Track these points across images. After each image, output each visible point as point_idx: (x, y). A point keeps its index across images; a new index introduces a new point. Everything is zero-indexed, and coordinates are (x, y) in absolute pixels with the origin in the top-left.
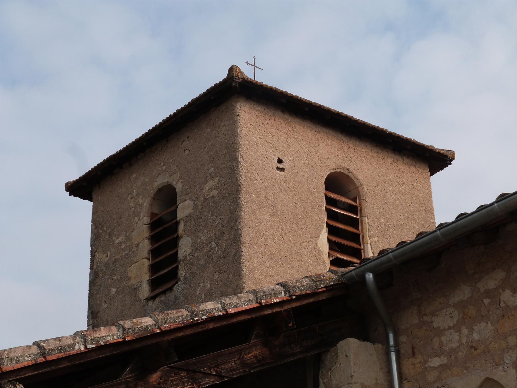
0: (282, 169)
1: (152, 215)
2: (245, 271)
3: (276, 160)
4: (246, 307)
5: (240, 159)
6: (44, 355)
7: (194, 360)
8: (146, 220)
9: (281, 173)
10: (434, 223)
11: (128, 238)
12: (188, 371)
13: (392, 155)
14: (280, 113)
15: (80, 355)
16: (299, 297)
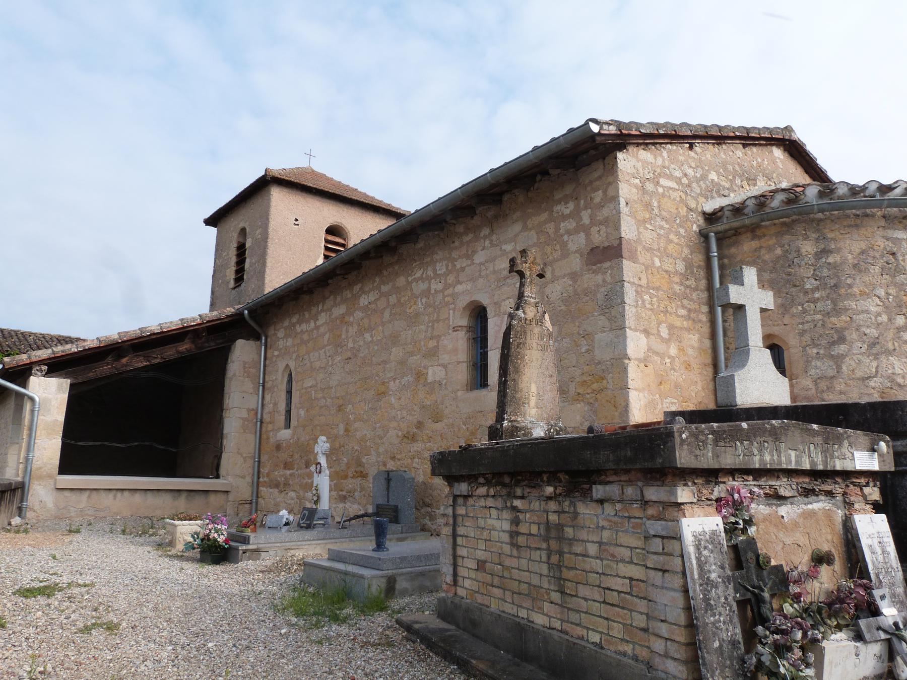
0: (298, 225)
1: (239, 242)
2: (266, 281)
3: (294, 219)
4: (175, 328)
5: (270, 220)
6: (54, 354)
7: (147, 352)
8: (235, 245)
9: (297, 227)
10: (263, 290)
11: (228, 254)
12: (144, 357)
13: (373, 214)
14: (300, 193)
15: (75, 353)
16: (208, 322)
